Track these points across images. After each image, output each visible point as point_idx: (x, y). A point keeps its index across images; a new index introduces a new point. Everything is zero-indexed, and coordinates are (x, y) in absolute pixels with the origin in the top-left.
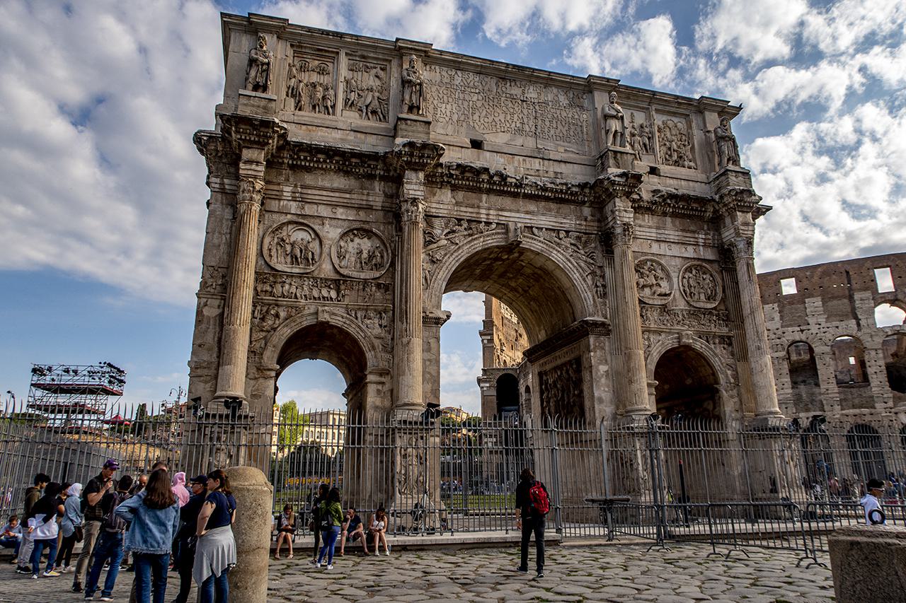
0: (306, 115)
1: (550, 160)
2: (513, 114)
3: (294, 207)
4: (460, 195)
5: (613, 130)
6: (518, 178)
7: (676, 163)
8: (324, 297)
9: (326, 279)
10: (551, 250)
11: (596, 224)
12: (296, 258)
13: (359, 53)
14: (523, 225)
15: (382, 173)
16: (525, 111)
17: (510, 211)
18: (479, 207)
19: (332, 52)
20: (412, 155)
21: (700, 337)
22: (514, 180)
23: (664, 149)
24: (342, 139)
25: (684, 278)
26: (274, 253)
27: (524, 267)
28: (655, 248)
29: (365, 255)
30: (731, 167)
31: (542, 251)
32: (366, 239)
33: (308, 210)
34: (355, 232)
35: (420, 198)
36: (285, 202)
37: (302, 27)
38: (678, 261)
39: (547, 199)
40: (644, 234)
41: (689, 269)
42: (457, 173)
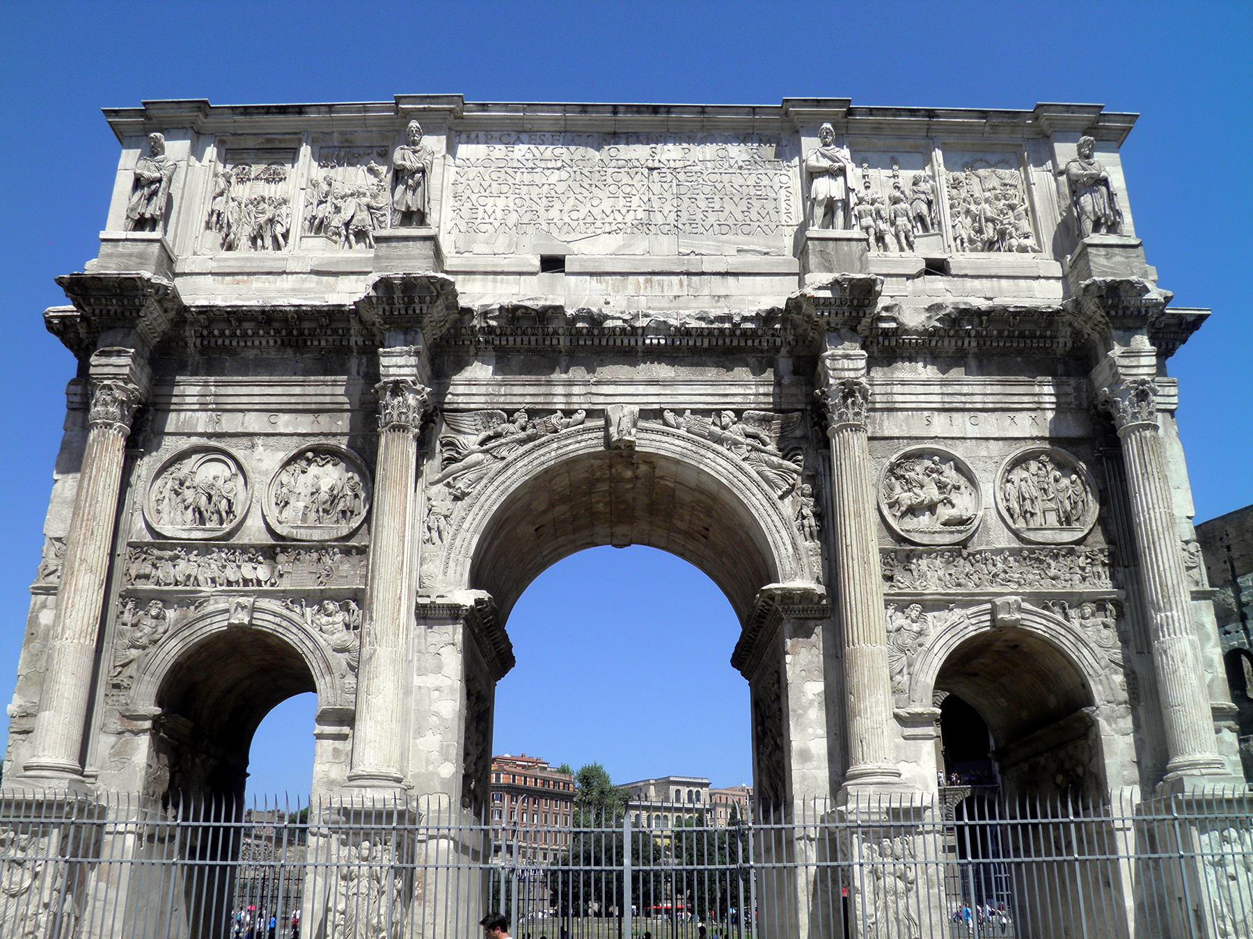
1: (703, 273)
2: (628, 196)
3: (202, 422)
5: (821, 197)
6: (627, 317)
7: (990, 246)
8: (246, 582)
9: (253, 546)
10: (702, 451)
12: (200, 513)
14: (637, 408)
15: (360, 343)
16: (656, 188)
17: (615, 383)
19: (291, 141)
21: (1046, 608)
22: (619, 323)
24: (293, 290)
25: (1008, 481)
26: (165, 506)
27: (673, 490)
28: (940, 425)
29: (324, 496)
30: (1095, 238)
31: (682, 455)
32: (329, 466)
33: (229, 423)
34: (310, 455)
35: (409, 379)
36: (189, 414)
40: (913, 398)
41: (1019, 462)
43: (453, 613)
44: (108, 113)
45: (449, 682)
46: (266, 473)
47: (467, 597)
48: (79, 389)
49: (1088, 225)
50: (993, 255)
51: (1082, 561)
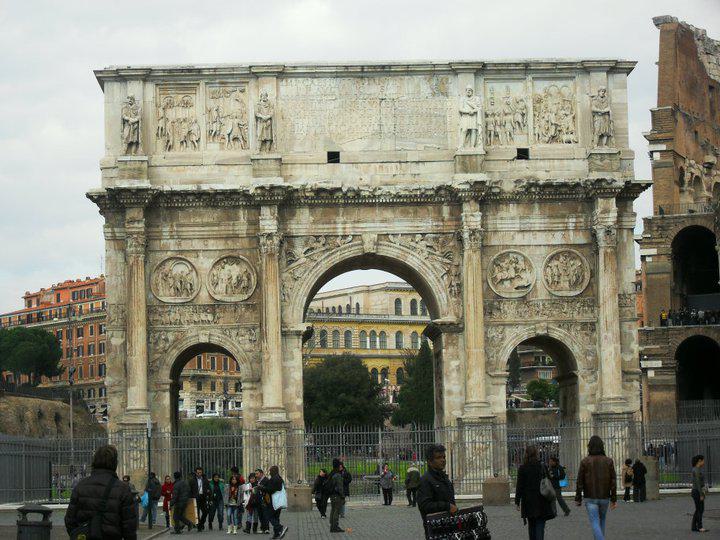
0: (179, 151)
3: (172, 244)
4: (319, 211)
5: (465, 130)
7: (553, 139)
11: (454, 223)
13: (217, 81)
16: (384, 111)
18: (335, 223)
20: (264, 196)
21: (560, 326)
22: (368, 193)
23: (543, 122)
29: (234, 280)
32: (235, 265)
33: (185, 245)
37: (164, 70)
38: (543, 250)
39: (403, 204)
42: (312, 194)
43: (298, 333)
44: (96, 72)
45: (297, 364)
46: (206, 269)
47: (303, 327)
48: (110, 230)
49: (596, 138)
50: (555, 145)
51: (578, 305)
